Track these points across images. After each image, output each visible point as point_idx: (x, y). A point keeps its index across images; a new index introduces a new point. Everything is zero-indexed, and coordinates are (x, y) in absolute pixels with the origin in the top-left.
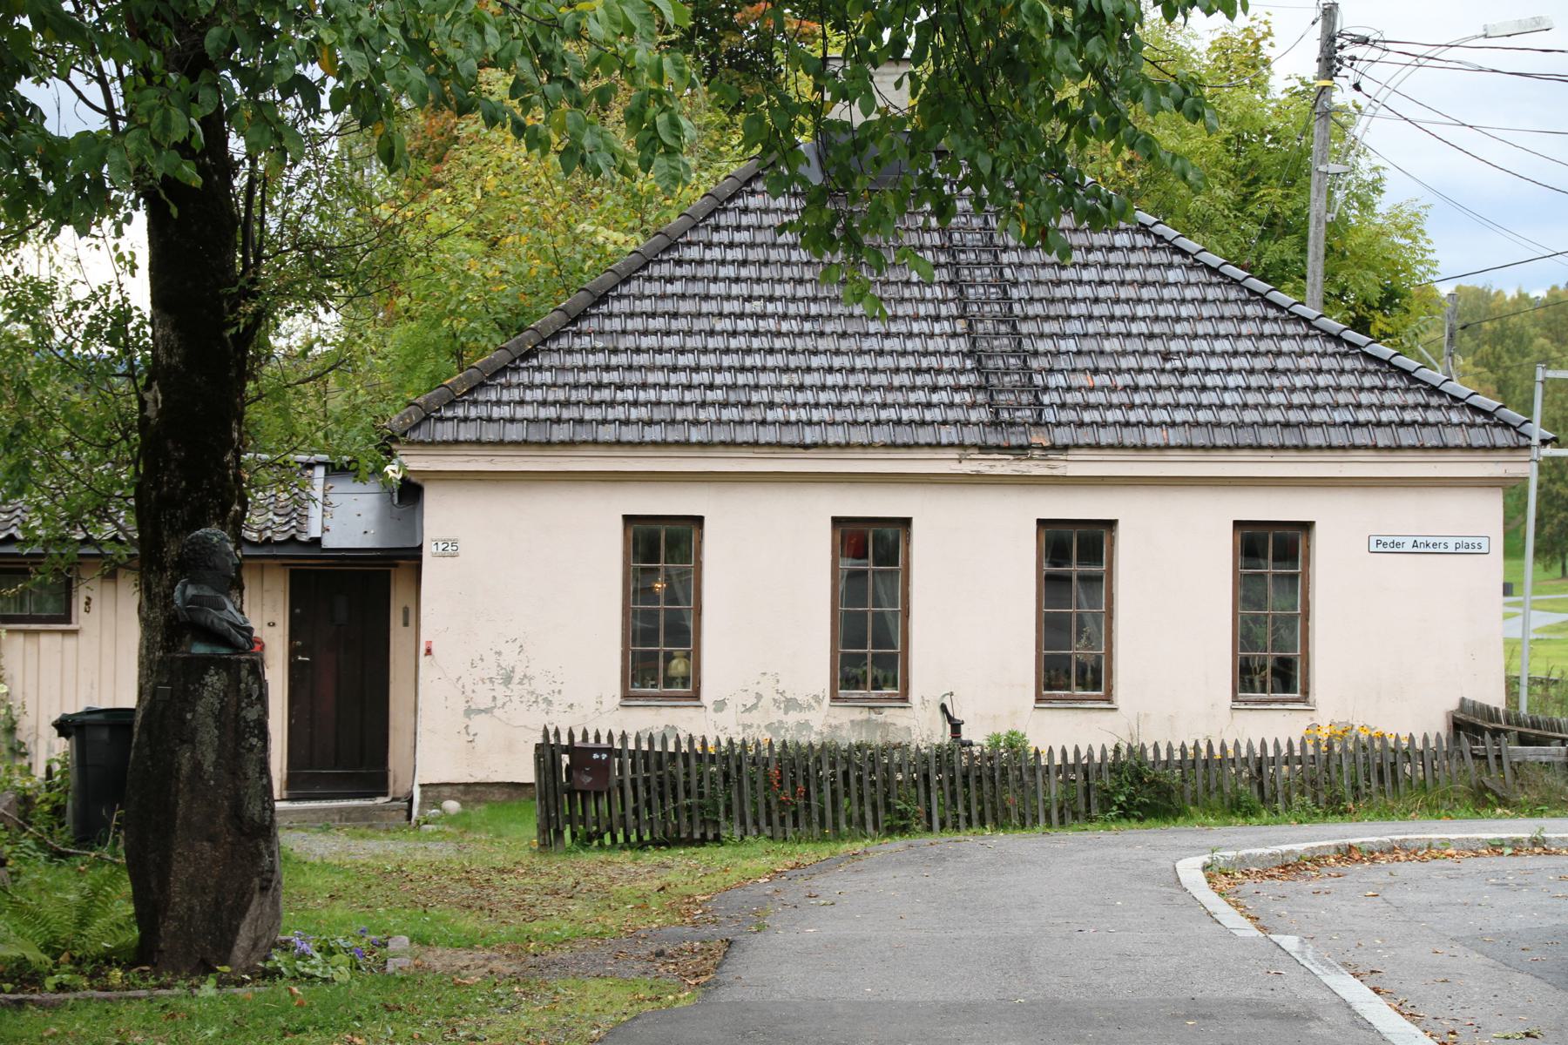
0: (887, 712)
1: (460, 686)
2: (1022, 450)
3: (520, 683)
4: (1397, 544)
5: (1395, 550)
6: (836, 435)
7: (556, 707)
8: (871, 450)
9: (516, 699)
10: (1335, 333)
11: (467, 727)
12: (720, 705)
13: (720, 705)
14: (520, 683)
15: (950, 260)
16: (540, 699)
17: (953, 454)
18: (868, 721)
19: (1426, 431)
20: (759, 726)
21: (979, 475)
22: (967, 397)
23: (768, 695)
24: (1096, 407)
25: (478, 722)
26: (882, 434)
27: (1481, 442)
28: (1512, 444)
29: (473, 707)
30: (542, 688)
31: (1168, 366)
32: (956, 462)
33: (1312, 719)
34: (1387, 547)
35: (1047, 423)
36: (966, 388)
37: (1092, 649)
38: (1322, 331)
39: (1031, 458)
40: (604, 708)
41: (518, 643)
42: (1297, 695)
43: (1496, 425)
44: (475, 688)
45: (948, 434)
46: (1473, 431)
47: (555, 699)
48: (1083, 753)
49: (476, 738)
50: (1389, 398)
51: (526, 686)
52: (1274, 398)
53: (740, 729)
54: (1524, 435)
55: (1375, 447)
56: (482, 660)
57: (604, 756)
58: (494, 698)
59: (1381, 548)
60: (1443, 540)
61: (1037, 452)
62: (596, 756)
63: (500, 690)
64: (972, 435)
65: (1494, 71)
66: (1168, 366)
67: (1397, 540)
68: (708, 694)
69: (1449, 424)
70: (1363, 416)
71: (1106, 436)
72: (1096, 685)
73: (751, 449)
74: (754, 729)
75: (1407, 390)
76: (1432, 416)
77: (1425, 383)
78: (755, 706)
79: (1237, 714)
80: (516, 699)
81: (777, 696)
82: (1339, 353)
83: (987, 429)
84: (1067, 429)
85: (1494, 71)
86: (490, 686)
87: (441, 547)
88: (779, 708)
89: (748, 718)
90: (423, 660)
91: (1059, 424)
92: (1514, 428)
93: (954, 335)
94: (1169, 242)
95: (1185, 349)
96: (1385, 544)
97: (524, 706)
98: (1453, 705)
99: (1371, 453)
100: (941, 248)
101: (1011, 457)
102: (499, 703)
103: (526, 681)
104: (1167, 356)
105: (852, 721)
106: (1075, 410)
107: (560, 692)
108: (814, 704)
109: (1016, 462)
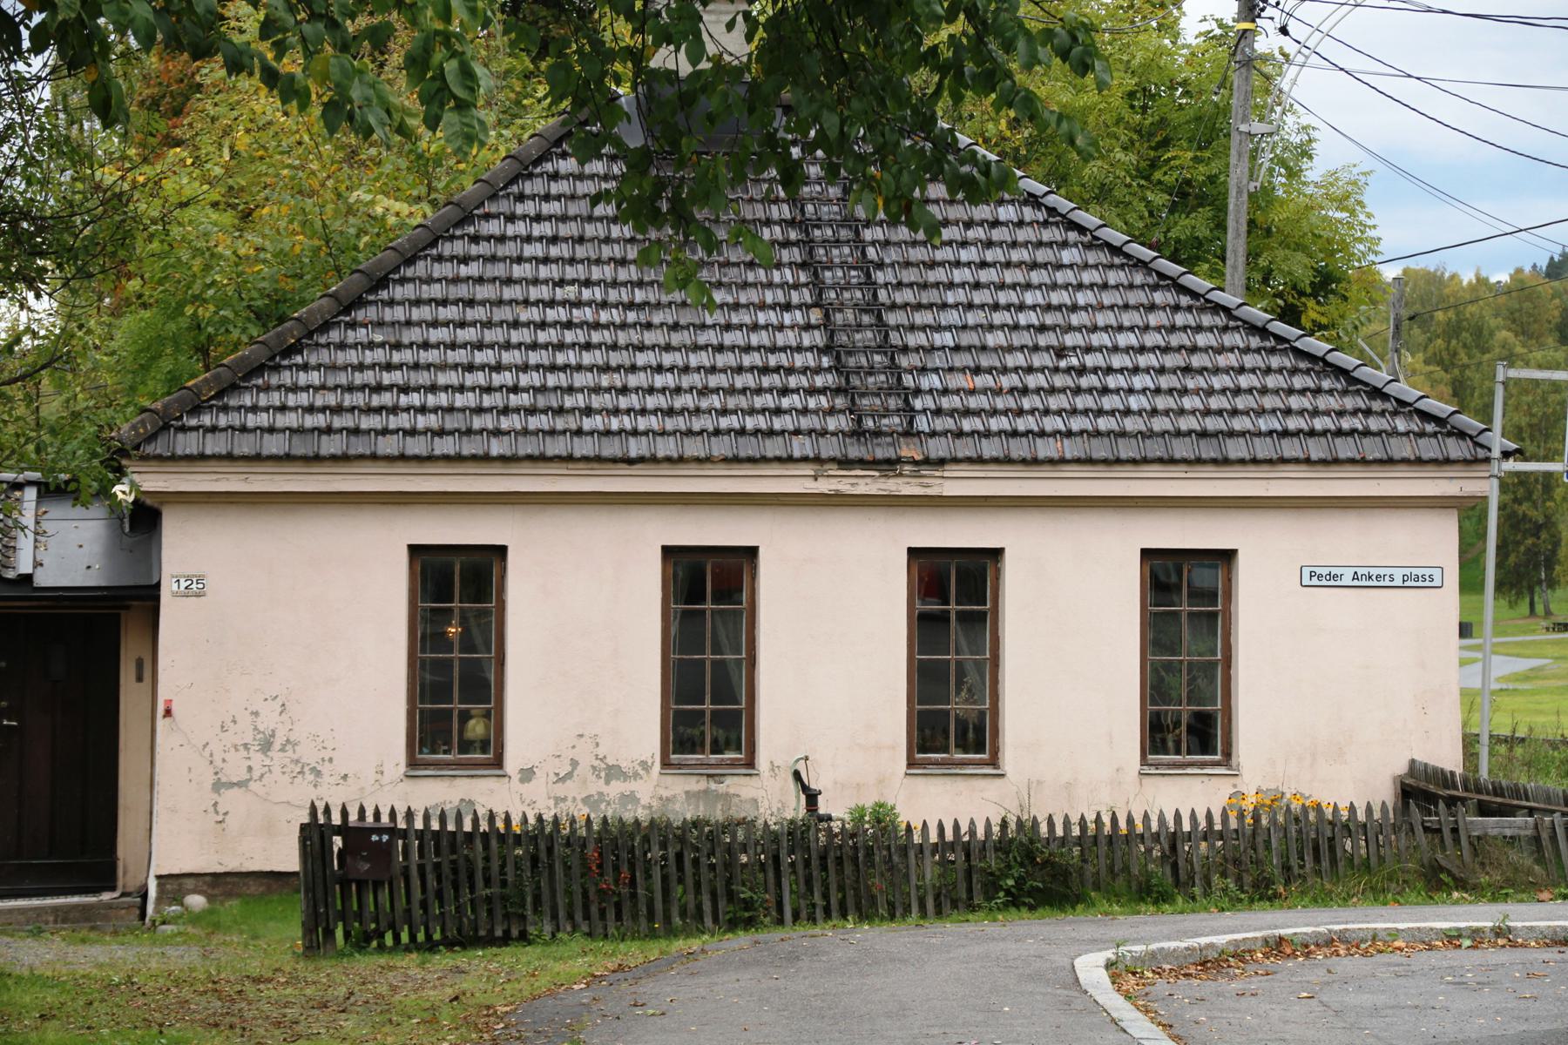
0: (729, 781)
1: (207, 753)
2: (889, 465)
3: (282, 750)
4: (1335, 576)
5: (1332, 583)
6: (666, 447)
7: (326, 778)
8: (709, 466)
9: (277, 769)
10: (1259, 324)
11: (215, 804)
12: (527, 775)
13: (527, 775)
14: (282, 750)
15: (802, 236)
16: (306, 769)
17: (808, 470)
19: (1367, 441)
20: (574, 799)
22: (823, 402)
23: (586, 761)
24: (977, 413)
25: (229, 798)
26: (721, 447)
27: (1432, 455)
28: (1469, 457)
29: (224, 780)
30: (309, 754)
31: (1063, 364)
32: (811, 480)
33: (1235, 786)
35: (919, 433)
36: (822, 391)
37: (974, 703)
38: (1245, 322)
39: (901, 475)
40: (386, 779)
41: (279, 701)
42: (1218, 757)
43: (1449, 434)
44: (227, 756)
45: (801, 446)
46: (1423, 442)
47: (326, 769)
48: (964, 828)
49: (227, 817)
50: (1323, 402)
51: (290, 753)
52: (1188, 403)
53: (552, 802)
54: (1482, 446)
55: (1308, 461)
56: (234, 722)
57: (385, 838)
58: (250, 769)
59: (1315, 581)
60: (1388, 571)
61: (908, 468)
62: (375, 838)
63: (257, 759)
64: (829, 448)
66: (1063, 364)
67: (1334, 571)
68: (514, 759)
69: (1394, 433)
70: (1293, 423)
71: (990, 448)
72: (980, 748)
73: (565, 465)
74: (569, 803)
75: (1345, 393)
76: (1374, 424)
77: (1366, 384)
78: (569, 775)
79: (1146, 780)
80: (277, 769)
82: (1264, 349)
83: (847, 440)
84: (943, 439)
86: (245, 754)
87: (183, 584)
88: (598, 777)
89: (560, 790)
90: (161, 723)
91: (933, 434)
92: (1471, 437)
93: (808, 327)
94: (1063, 216)
95: (1082, 343)
96: (1320, 577)
97: (287, 778)
98: (1401, 768)
99: (1303, 467)
100: (791, 223)
101: (876, 474)
102: (256, 775)
103: (289, 747)
104: (1061, 352)
105: (687, 793)
106: (952, 416)
107: (331, 760)
108: (642, 772)
109: (883, 480)
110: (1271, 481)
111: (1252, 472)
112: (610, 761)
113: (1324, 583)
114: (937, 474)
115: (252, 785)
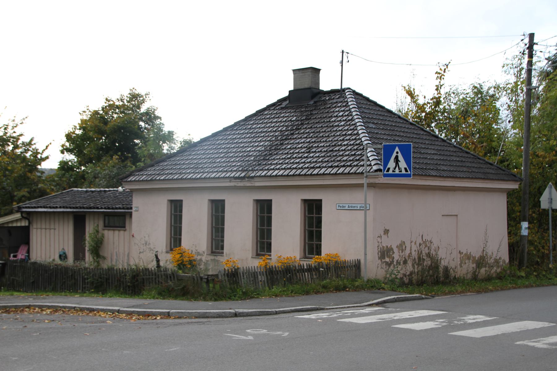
0: (219, 257)
5: (343, 208)
14: (148, 245)
18: (214, 259)
21: (235, 186)
34: (342, 208)
58: (144, 249)
65: (556, 36)
67: (344, 205)
81: (196, 251)
85: (556, 36)
96: (340, 207)
105: (211, 259)
110: (325, 180)
111: (318, 177)
112: (198, 251)
113: (341, 208)
114: (253, 180)
115: (144, 253)
